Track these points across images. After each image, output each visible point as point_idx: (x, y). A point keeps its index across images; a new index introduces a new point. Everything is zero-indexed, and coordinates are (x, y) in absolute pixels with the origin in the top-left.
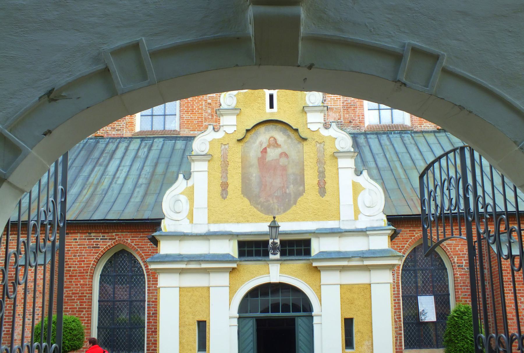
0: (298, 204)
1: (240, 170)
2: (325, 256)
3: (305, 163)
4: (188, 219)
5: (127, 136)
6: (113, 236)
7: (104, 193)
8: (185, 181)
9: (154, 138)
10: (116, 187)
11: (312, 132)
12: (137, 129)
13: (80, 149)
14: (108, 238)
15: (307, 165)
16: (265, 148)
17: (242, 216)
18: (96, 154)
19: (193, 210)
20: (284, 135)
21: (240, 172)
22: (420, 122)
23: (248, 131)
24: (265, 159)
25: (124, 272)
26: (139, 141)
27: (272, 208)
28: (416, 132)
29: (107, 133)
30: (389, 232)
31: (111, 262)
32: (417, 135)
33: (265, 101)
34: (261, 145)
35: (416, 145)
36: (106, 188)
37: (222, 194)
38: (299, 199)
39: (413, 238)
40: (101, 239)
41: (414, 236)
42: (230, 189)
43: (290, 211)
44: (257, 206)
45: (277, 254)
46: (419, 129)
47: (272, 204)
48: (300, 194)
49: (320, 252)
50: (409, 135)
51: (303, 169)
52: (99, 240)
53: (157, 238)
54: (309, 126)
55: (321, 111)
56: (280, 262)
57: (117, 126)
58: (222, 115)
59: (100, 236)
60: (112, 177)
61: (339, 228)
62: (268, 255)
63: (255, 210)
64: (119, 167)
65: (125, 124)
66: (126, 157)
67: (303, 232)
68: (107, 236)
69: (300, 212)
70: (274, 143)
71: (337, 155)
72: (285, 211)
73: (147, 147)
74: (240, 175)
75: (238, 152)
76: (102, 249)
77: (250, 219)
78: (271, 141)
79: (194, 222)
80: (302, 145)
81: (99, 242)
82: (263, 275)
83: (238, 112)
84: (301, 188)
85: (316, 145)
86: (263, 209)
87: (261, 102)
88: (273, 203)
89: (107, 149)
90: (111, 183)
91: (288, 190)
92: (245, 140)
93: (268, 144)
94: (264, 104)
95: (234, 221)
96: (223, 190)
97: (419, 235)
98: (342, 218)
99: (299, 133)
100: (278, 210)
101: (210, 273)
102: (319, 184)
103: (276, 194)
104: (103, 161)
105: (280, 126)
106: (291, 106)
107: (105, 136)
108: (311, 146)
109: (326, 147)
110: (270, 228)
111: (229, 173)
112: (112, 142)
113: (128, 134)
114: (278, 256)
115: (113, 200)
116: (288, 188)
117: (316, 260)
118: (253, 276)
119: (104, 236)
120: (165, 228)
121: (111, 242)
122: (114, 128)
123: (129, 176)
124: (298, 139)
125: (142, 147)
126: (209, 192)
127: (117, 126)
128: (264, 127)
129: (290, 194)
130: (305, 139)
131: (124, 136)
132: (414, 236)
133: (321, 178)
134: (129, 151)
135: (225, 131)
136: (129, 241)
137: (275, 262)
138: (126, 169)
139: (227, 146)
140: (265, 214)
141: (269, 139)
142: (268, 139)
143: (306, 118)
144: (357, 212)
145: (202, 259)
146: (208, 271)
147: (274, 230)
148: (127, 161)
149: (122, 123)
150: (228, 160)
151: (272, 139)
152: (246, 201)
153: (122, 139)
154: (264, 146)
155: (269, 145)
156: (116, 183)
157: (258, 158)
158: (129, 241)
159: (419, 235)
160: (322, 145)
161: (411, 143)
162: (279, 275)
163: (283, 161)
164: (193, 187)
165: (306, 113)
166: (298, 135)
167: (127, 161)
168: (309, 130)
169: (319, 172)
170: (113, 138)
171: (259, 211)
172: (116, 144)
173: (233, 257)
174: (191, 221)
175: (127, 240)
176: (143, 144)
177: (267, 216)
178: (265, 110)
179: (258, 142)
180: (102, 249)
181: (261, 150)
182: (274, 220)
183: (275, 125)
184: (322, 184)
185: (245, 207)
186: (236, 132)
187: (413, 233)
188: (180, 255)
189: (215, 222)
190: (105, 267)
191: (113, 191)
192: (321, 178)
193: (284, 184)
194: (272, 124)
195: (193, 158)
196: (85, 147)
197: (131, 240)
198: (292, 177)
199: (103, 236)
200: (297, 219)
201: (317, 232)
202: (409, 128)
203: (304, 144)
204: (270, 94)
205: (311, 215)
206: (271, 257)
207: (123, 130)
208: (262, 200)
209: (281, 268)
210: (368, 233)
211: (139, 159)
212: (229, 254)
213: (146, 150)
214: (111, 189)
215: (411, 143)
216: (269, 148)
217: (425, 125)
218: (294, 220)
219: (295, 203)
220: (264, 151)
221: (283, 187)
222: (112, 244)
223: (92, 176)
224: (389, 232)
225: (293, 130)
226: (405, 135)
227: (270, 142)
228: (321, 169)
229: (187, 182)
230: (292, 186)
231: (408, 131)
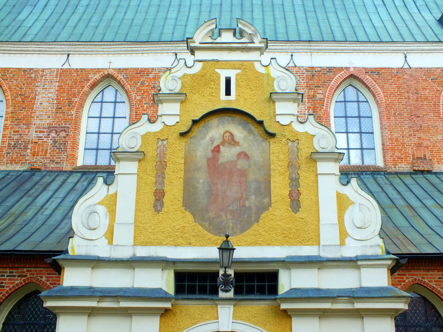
0: (261, 221)
1: (181, 174)
2: (299, 295)
3: (272, 167)
4: (106, 238)
5: (67, 170)
6: (24, 272)
7: (25, 223)
8: (106, 187)
9: (97, 172)
10: (41, 218)
11: (282, 127)
12: (80, 163)
13: (10, 180)
14: (17, 274)
15: (275, 170)
16: (218, 146)
17: (182, 237)
18: (28, 186)
19: (113, 227)
20: (244, 130)
21: (182, 176)
22: (394, 163)
23: (195, 122)
24: (218, 161)
25: (35, 319)
26: (79, 175)
27: (225, 227)
28: (390, 173)
29: (45, 165)
30: (389, 262)
31: (19, 307)
32: (391, 176)
33: (220, 86)
34: (212, 141)
35: (392, 185)
36: (29, 218)
37: (155, 206)
38: (263, 215)
39: (403, 284)
40: (8, 276)
41: (404, 281)
42: (165, 199)
43: (250, 231)
44: (204, 223)
45: (230, 290)
46: (393, 170)
47: (225, 221)
48: (265, 208)
49: (292, 289)
50: (383, 176)
51: (270, 176)
52: (5, 277)
53: (60, 263)
54: (278, 118)
55: (295, 100)
56: (234, 302)
57: (57, 158)
58: (161, 102)
59: (6, 273)
60: (39, 207)
61: (319, 256)
62: (217, 293)
63: (201, 228)
64: (50, 198)
65: (66, 157)
66: (61, 190)
67: (268, 260)
68: (16, 272)
69: (263, 233)
70: (230, 139)
71: (315, 156)
72: (243, 230)
73: (87, 180)
74: (181, 180)
75: (180, 150)
76: (8, 289)
77: (193, 241)
78: (226, 136)
79: (114, 243)
80: (268, 143)
81: (5, 280)
82: (208, 320)
83: (183, 98)
84: (266, 200)
85: (288, 143)
86: (211, 227)
87: (214, 87)
88: (227, 219)
89: (42, 181)
90: (36, 214)
91: (248, 203)
92: (190, 134)
93: (222, 140)
94: (218, 89)
95: (171, 243)
96: (157, 200)
97: (410, 280)
98: (322, 243)
99: (265, 127)
100: (233, 229)
101: (131, 316)
102: (290, 195)
103: (231, 208)
104: (33, 193)
105: (238, 118)
106: (253, 93)
107: (43, 169)
108: (280, 145)
109: (300, 146)
110: (221, 251)
111: (166, 178)
112: (49, 175)
113: (67, 167)
114: (231, 294)
115: (32, 231)
116: (247, 199)
117: (286, 299)
118: (194, 322)
119: (12, 272)
120: (73, 250)
121: (21, 279)
122: (53, 161)
123: (60, 208)
124: (263, 136)
125: (81, 180)
126: (137, 202)
127: (57, 158)
128: (218, 118)
129: (250, 208)
130: (272, 135)
131: (64, 169)
132: (404, 281)
133: (293, 188)
134: (66, 184)
135: (164, 122)
136: (44, 279)
137: (226, 302)
138: (58, 201)
139: (165, 142)
140: (215, 235)
141: (224, 134)
142: (222, 134)
143: (275, 109)
144: (343, 234)
145: (121, 294)
146: (129, 312)
147: (226, 254)
148: (61, 194)
149: (62, 156)
150: (166, 160)
151: (228, 134)
152: (189, 216)
153: (61, 172)
154: (216, 143)
155: (223, 143)
156: (42, 214)
157: (208, 158)
158: (44, 279)
159: (410, 280)
160: (296, 144)
161: (386, 184)
162: (231, 320)
163: (242, 164)
164: (116, 194)
165: (274, 102)
166: (263, 129)
167: (61, 194)
168: (278, 123)
169: (292, 179)
170: (52, 171)
171: (206, 230)
172: (53, 177)
173: (166, 293)
174: (110, 242)
175: (42, 277)
176: (84, 178)
177: (218, 237)
178: (219, 97)
179: (208, 138)
180: (8, 289)
181: (212, 149)
182: (227, 239)
183: (232, 117)
184: (294, 195)
185: (187, 225)
186: (179, 124)
187: (403, 278)
188: (91, 288)
189: (145, 244)
190: (10, 313)
191: (36, 221)
192: (293, 188)
193: (242, 194)
194: (227, 115)
195: (118, 156)
196: (17, 179)
197: (46, 277)
198: (253, 186)
199: (10, 272)
200: (260, 242)
201: (287, 260)
202: (382, 168)
203: (271, 142)
204: (226, 77)
205: (280, 237)
206: (222, 294)
207: (63, 163)
208: (211, 215)
209: (234, 311)
210: (359, 263)
211: (76, 192)
212: (161, 289)
213: (85, 183)
214: (35, 219)
215: (386, 184)
216: (223, 146)
217: (399, 166)
218: (255, 243)
219: (257, 220)
220: (217, 150)
221: (241, 198)
222: (21, 283)
223: (16, 206)
224: (389, 262)
225: (256, 123)
226: (379, 176)
227: (225, 138)
228: (294, 176)
229: (108, 189)
230: (253, 197)
231: (381, 172)
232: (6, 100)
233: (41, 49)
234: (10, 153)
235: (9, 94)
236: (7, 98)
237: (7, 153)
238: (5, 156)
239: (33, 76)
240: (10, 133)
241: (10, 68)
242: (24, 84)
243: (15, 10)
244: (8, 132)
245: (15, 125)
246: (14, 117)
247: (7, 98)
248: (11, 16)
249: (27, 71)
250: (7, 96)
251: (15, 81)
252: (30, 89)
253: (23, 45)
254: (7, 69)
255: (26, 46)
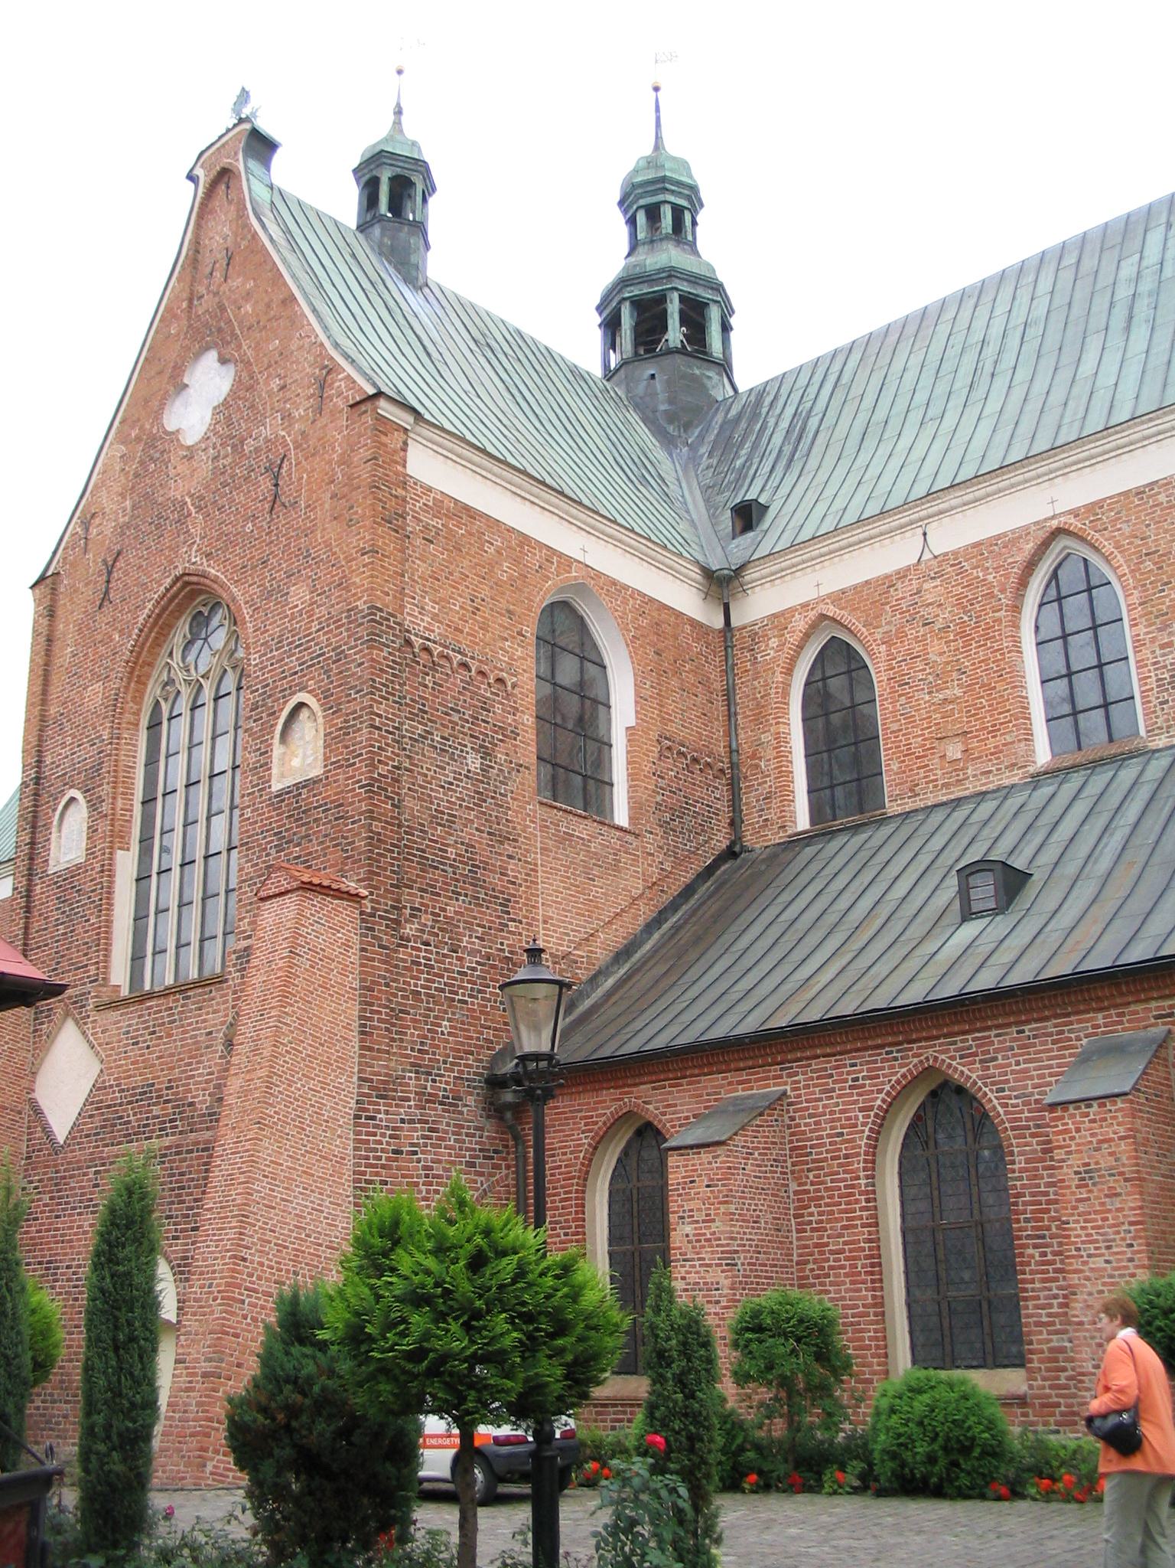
232: (1120, 577)
233: (1160, 427)
234: (1167, 702)
235: (1122, 561)
236: (1120, 572)
237: (1161, 703)
238: (1159, 713)
239: (1162, 498)
240: (1153, 652)
241: (1104, 500)
242: (1148, 526)
243: (1067, 358)
244: (1146, 653)
245: (1160, 630)
246: (1151, 613)
247: (1120, 572)
248: (1064, 375)
249: (1144, 492)
250: (1119, 567)
251: (1124, 526)
252: (1166, 531)
253: (1117, 433)
254: (1099, 504)
255: (1123, 434)
